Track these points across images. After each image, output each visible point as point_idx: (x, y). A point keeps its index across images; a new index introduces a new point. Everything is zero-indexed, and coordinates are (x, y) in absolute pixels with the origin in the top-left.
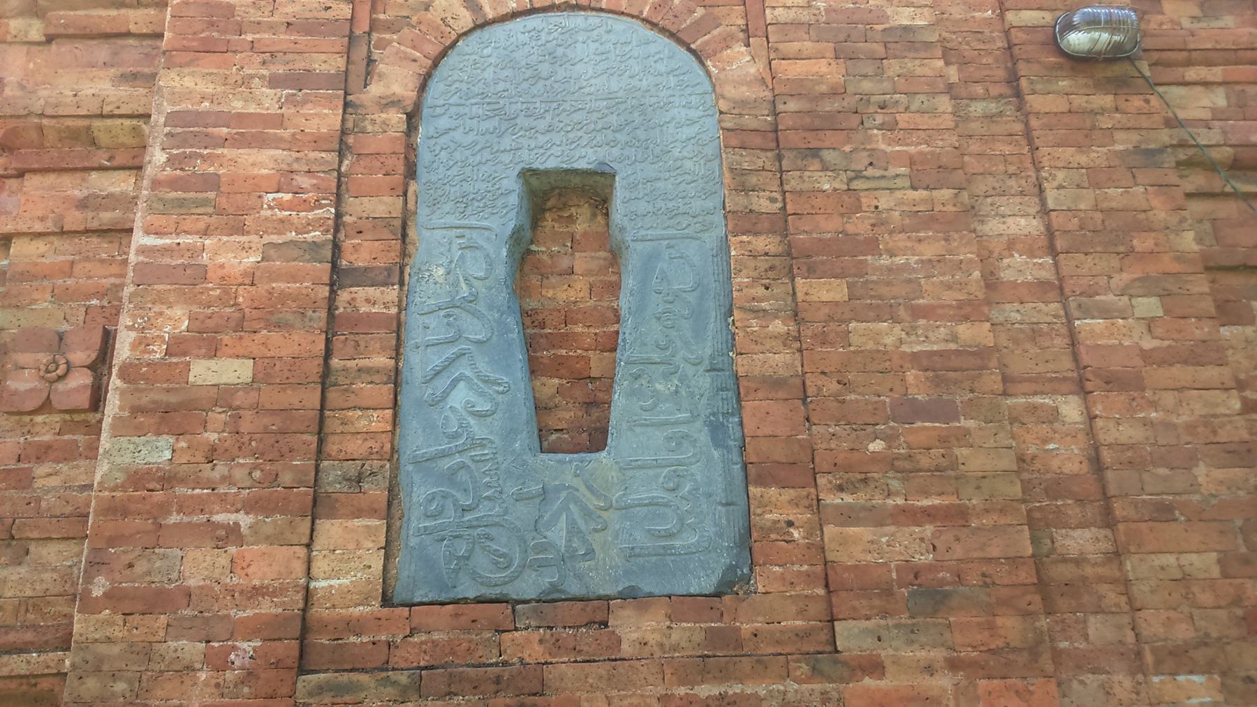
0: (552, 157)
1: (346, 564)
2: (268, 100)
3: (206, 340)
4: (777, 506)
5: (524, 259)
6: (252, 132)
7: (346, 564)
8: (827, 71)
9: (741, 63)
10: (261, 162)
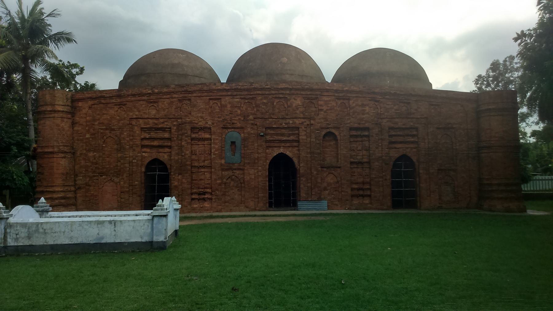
0: (232, 140)
1: (223, 162)
2: (217, 137)
4: (243, 159)
5: (231, 146)
6: (217, 139)
7: (223, 162)
9: (242, 135)
10: (217, 141)
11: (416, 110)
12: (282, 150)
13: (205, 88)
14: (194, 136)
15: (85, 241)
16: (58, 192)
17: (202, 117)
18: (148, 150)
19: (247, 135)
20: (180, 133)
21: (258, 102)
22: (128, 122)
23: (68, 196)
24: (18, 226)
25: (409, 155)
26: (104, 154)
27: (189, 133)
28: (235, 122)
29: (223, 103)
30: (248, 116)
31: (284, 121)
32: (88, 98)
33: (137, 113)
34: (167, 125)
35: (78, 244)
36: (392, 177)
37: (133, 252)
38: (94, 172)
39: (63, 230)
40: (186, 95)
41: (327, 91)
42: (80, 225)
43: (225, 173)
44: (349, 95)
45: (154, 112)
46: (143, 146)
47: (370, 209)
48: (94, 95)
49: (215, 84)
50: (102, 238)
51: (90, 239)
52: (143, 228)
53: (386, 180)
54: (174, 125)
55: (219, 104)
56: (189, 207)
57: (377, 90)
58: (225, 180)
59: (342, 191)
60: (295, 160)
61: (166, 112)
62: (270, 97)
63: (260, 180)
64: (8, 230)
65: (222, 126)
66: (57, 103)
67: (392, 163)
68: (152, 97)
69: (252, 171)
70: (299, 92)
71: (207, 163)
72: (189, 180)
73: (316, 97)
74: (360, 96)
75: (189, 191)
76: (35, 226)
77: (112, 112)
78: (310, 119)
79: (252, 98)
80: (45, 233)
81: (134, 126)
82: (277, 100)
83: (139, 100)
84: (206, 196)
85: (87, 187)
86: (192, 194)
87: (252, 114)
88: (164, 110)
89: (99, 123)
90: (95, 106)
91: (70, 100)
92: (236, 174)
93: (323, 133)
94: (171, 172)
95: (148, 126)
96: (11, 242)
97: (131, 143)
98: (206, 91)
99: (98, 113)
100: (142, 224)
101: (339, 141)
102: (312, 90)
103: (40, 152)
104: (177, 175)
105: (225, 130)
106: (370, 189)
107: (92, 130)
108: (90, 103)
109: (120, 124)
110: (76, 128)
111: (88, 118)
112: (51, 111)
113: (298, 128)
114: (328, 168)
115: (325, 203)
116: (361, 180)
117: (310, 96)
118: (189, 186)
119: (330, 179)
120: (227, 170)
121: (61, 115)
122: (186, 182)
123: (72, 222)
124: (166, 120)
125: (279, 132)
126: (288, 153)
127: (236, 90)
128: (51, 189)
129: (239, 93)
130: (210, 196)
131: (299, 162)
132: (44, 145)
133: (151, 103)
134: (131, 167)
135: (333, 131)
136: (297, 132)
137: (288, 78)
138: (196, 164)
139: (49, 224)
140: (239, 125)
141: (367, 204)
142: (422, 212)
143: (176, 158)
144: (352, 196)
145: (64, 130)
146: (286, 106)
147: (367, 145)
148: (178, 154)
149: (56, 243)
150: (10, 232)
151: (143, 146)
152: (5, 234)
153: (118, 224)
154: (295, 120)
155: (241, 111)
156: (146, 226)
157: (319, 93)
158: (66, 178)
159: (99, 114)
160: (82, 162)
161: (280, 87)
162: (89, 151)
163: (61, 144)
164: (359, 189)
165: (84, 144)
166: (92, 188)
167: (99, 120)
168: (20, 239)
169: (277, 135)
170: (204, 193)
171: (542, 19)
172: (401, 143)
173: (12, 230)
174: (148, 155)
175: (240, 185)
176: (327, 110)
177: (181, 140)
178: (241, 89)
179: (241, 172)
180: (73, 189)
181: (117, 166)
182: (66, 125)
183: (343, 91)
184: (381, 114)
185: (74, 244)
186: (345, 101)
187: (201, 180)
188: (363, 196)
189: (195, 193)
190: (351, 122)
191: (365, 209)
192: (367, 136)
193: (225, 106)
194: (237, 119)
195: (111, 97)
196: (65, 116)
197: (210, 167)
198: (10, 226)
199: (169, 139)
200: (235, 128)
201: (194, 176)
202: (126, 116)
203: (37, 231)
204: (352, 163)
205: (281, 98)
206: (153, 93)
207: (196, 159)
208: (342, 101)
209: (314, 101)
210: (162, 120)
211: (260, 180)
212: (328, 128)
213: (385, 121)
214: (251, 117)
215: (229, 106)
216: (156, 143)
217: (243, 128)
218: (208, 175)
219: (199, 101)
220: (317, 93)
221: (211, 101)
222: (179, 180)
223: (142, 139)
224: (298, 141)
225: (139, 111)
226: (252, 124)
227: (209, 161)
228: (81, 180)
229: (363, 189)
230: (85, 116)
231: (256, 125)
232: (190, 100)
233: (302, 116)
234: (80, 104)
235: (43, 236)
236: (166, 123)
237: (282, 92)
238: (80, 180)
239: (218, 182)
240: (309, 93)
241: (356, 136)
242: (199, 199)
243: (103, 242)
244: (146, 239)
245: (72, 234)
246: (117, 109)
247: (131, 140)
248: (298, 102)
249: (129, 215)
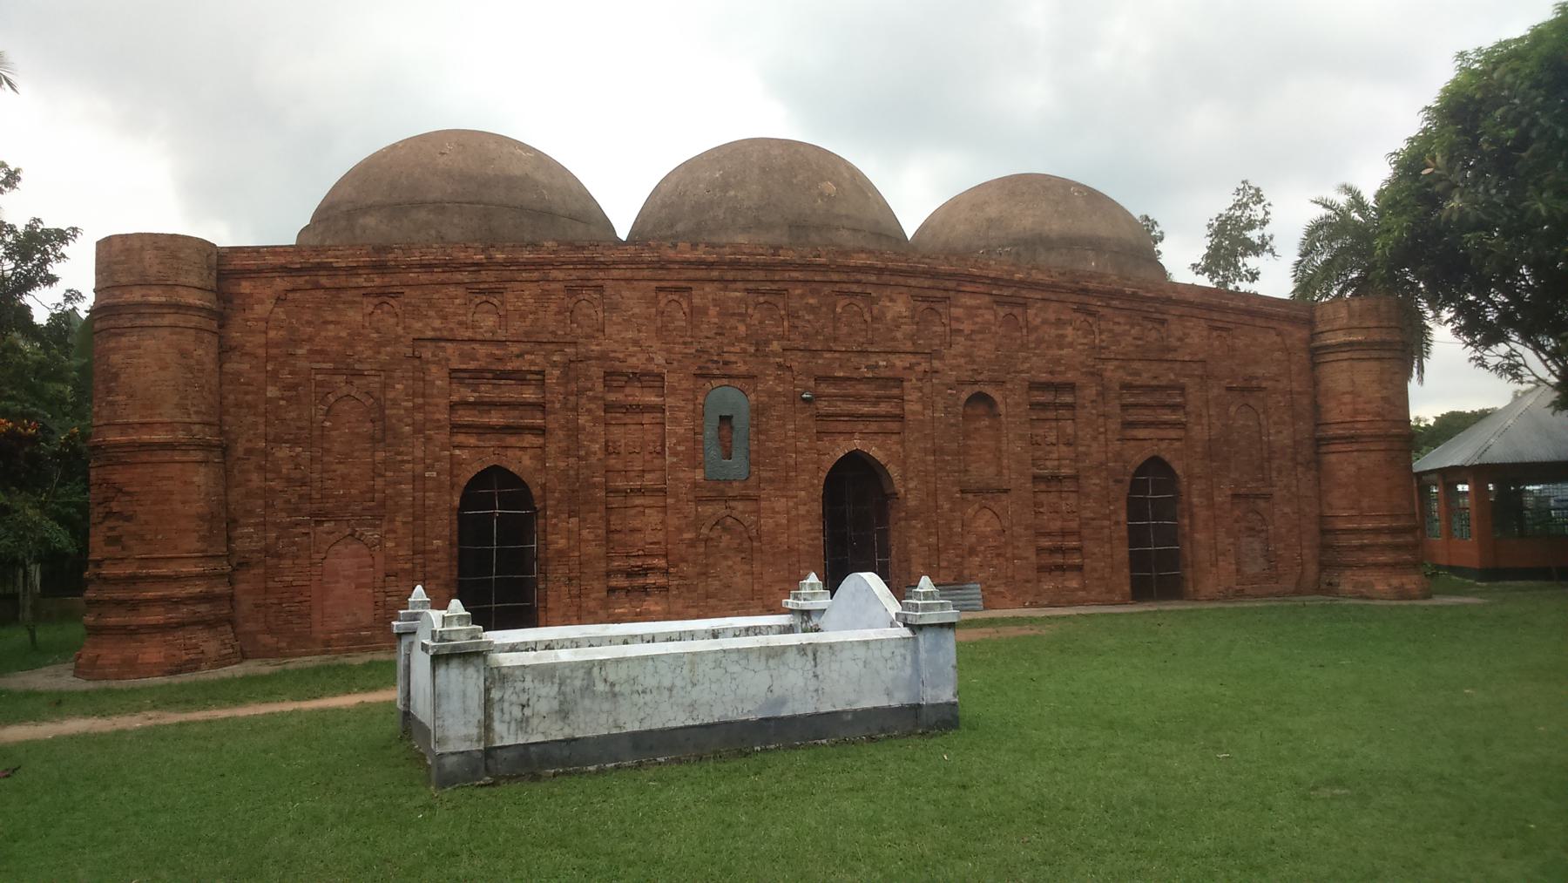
3: (678, 443)
4: (754, 469)
6: (681, 409)
7: (699, 475)
8: (764, 399)
9: (752, 397)
10: (682, 415)
11: (1180, 339)
12: (857, 444)
13: (647, 255)
14: (612, 397)
15: (733, 715)
16: (190, 577)
17: (636, 342)
18: (472, 441)
19: (764, 399)
20: (573, 387)
21: (794, 304)
22: (409, 352)
23: (217, 590)
24: (529, 678)
25: (1167, 458)
26: (327, 451)
27: (599, 387)
28: (733, 359)
29: (697, 301)
30: (767, 343)
31: (862, 362)
32: (274, 269)
33: (437, 323)
34: (532, 363)
35: (714, 725)
36: (1131, 516)
37: (871, 739)
38: (297, 510)
39: (667, 683)
40: (590, 274)
41: (974, 279)
42: (718, 664)
43: (707, 510)
44: (1024, 293)
45: (489, 321)
46: (456, 428)
47: (1082, 602)
48: (297, 259)
49: (675, 246)
50: (782, 702)
51: (749, 706)
52: (890, 664)
53: (1117, 523)
54: (554, 365)
55: (685, 305)
56: (601, 612)
57: (1092, 285)
58: (704, 531)
59: (1015, 557)
60: (894, 471)
61: (528, 322)
62: (827, 289)
63: (803, 527)
64: (495, 694)
65: (693, 369)
66: (182, 280)
67: (1128, 479)
68: (483, 275)
69: (781, 504)
70: (901, 280)
71: (650, 480)
72: (601, 532)
73: (945, 294)
74: (1053, 297)
75: (602, 566)
76: (581, 673)
77: (354, 316)
78: (932, 355)
79: (778, 292)
80: (615, 695)
81: (428, 362)
82: (842, 302)
83: (443, 284)
84: (651, 580)
85: (275, 561)
86: (608, 574)
87: (781, 338)
88: (523, 316)
89: (311, 352)
90: (298, 295)
91: (214, 273)
92: (735, 513)
93: (964, 396)
94: (545, 508)
95: (472, 365)
96: (506, 735)
97: (419, 416)
98: (651, 265)
99: (307, 317)
100: (887, 653)
101: (1003, 418)
102: (933, 274)
103: (116, 446)
104: (564, 516)
105: (701, 381)
106: (1079, 549)
107: (285, 375)
108: (281, 284)
109: (383, 357)
110: (228, 367)
111: (272, 334)
112: (160, 305)
114: (978, 492)
115: (975, 590)
116: (1056, 525)
117: (930, 293)
118: (601, 551)
119: (984, 523)
120: (710, 500)
121: (195, 320)
122: (591, 537)
123: (694, 654)
124: (528, 347)
125: (851, 391)
126: (875, 452)
127: (734, 265)
128: (164, 571)
129: (739, 275)
130: (662, 581)
131: (904, 479)
132: (135, 419)
133: (482, 292)
134: (419, 494)
135: (988, 390)
136: (896, 392)
137: (845, 238)
138: (620, 483)
139: (624, 665)
140: (742, 368)
141: (1075, 590)
142: (1197, 605)
143: (562, 465)
144: (1041, 569)
145: (202, 371)
146: (868, 317)
147: (1070, 430)
148: (566, 453)
149: (645, 727)
150: (502, 699)
151: (456, 428)
152: (488, 703)
153: (824, 656)
154: (893, 358)
155: (748, 327)
156: (899, 658)
157: (950, 284)
158: (210, 530)
159: (309, 323)
160: (254, 476)
161: (852, 262)
162: (278, 440)
163: (195, 418)
164: (1053, 551)
165: (261, 420)
166: (287, 563)
167: (310, 339)
168: (535, 722)
169: (845, 398)
170: (646, 571)
171: (1425, 130)
172: (1147, 425)
173: (509, 692)
174: (473, 458)
175: (746, 545)
177: (575, 409)
178: (748, 264)
179: (751, 506)
181: (372, 490)
182: (204, 353)
183: (1010, 283)
185: (700, 726)
186: (1016, 311)
187: (633, 530)
188: (1061, 568)
189: (620, 571)
190: (1031, 368)
191: (1071, 604)
192: (1071, 407)
193: (704, 311)
194: (737, 349)
195: (352, 271)
196: (204, 323)
197: (664, 491)
198: (497, 677)
199: (541, 407)
200: (730, 377)
201: (612, 518)
202: (400, 330)
203: (588, 689)
204: (1036, 478)
205: (857, 294)
206: (490, 264)
207: (620, 467)
208: (1007, 310)
209: (939, 307)
210: (515, 349)
211: (803, 527)
212: (976, 382)
213: (1111, 366)
214: (775, 346)
215: (713, 311)
216: (495, 418)
217: (754, 377)
218: (654, 517)
219: (626, 293)
220: (949, 284)
221: (661, 295)
222: (569, 531)
223: (453, 407)
224: (901, 418)
225: (444, 318)
226: (780, 366)
227: (657, 475)
228: (249, 536)
229: (1062, 551)
230: (262, 325)
231: (790, 368)
232: (599, 288)
233: (909, 346)
234: (246, 287)
235: (606, 706)
236: (527, 357)
237: (859, 276)
238: (248, 539)
239: (687, 536)
240: (927, 283)
241: (1044, 406)
242: (628, 591)
243: (786, 712)
244: (899, 699)
245: (695, 693)
246: (370, 309)
247: (416, 408)
248: (898, 307)
249: (692, 635)
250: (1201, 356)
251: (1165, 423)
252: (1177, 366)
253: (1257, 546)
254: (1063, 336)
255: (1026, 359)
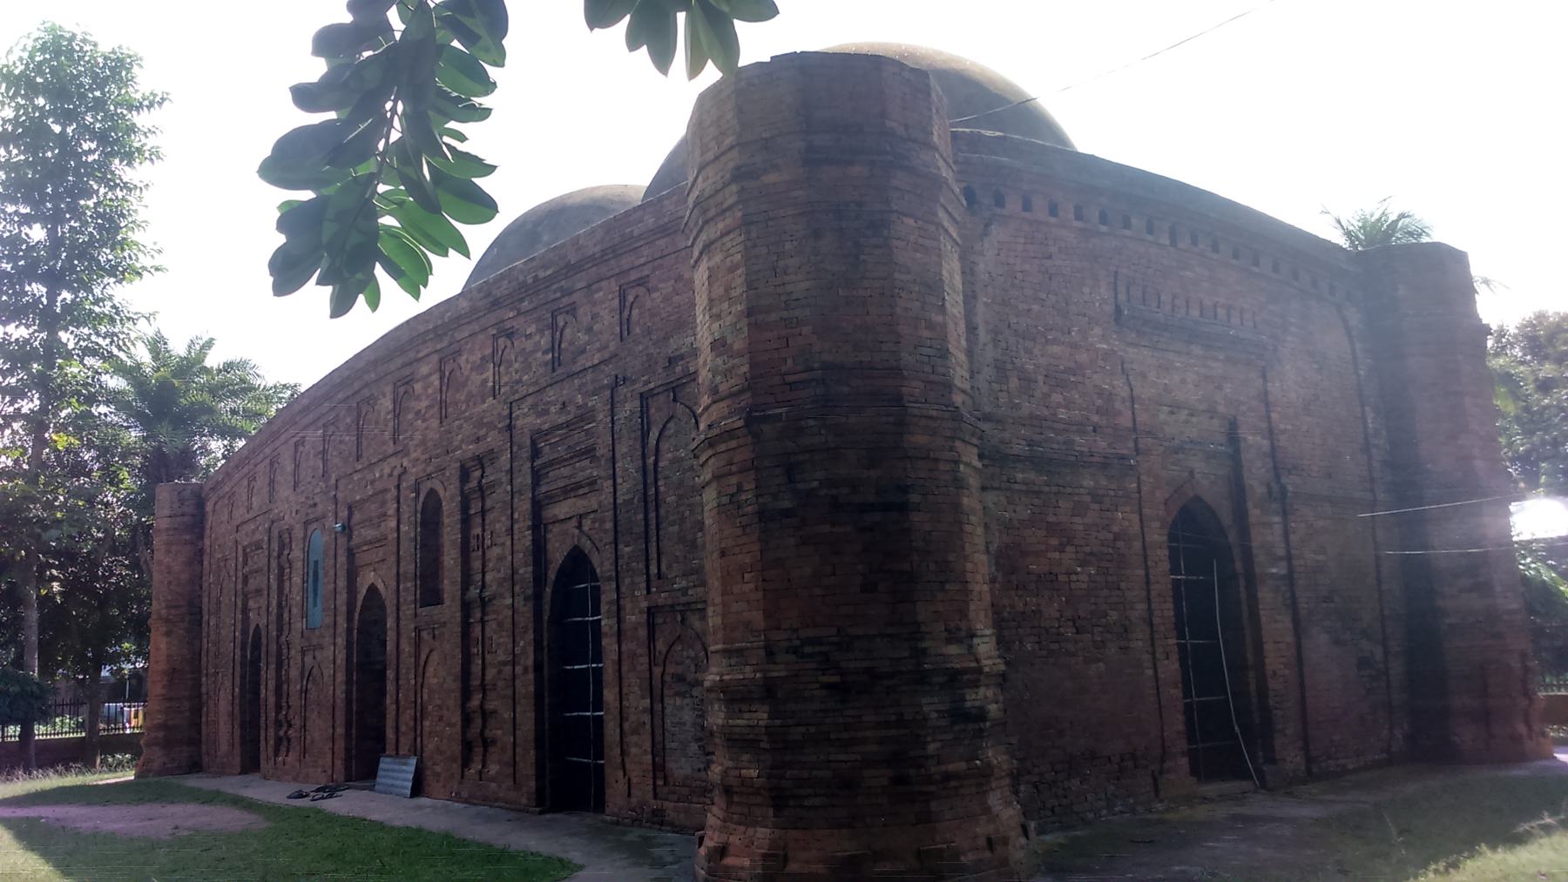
44: (458, 336)
113: (386, 491)
126: (380, 586)
176: (428, 408)
180: (187, 704)
184: (518, 382)
190: (462, 441)
233: (391, 448)
240: (399, 361)
250: (612, 347)
251: (578, 486)
252: (589, 376)
253: (688, 716)
254: (485, 381)
255: (460, 427)
